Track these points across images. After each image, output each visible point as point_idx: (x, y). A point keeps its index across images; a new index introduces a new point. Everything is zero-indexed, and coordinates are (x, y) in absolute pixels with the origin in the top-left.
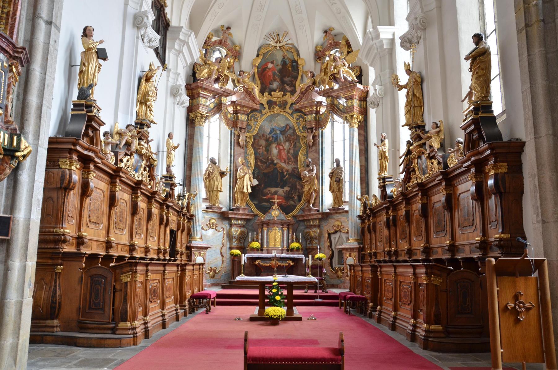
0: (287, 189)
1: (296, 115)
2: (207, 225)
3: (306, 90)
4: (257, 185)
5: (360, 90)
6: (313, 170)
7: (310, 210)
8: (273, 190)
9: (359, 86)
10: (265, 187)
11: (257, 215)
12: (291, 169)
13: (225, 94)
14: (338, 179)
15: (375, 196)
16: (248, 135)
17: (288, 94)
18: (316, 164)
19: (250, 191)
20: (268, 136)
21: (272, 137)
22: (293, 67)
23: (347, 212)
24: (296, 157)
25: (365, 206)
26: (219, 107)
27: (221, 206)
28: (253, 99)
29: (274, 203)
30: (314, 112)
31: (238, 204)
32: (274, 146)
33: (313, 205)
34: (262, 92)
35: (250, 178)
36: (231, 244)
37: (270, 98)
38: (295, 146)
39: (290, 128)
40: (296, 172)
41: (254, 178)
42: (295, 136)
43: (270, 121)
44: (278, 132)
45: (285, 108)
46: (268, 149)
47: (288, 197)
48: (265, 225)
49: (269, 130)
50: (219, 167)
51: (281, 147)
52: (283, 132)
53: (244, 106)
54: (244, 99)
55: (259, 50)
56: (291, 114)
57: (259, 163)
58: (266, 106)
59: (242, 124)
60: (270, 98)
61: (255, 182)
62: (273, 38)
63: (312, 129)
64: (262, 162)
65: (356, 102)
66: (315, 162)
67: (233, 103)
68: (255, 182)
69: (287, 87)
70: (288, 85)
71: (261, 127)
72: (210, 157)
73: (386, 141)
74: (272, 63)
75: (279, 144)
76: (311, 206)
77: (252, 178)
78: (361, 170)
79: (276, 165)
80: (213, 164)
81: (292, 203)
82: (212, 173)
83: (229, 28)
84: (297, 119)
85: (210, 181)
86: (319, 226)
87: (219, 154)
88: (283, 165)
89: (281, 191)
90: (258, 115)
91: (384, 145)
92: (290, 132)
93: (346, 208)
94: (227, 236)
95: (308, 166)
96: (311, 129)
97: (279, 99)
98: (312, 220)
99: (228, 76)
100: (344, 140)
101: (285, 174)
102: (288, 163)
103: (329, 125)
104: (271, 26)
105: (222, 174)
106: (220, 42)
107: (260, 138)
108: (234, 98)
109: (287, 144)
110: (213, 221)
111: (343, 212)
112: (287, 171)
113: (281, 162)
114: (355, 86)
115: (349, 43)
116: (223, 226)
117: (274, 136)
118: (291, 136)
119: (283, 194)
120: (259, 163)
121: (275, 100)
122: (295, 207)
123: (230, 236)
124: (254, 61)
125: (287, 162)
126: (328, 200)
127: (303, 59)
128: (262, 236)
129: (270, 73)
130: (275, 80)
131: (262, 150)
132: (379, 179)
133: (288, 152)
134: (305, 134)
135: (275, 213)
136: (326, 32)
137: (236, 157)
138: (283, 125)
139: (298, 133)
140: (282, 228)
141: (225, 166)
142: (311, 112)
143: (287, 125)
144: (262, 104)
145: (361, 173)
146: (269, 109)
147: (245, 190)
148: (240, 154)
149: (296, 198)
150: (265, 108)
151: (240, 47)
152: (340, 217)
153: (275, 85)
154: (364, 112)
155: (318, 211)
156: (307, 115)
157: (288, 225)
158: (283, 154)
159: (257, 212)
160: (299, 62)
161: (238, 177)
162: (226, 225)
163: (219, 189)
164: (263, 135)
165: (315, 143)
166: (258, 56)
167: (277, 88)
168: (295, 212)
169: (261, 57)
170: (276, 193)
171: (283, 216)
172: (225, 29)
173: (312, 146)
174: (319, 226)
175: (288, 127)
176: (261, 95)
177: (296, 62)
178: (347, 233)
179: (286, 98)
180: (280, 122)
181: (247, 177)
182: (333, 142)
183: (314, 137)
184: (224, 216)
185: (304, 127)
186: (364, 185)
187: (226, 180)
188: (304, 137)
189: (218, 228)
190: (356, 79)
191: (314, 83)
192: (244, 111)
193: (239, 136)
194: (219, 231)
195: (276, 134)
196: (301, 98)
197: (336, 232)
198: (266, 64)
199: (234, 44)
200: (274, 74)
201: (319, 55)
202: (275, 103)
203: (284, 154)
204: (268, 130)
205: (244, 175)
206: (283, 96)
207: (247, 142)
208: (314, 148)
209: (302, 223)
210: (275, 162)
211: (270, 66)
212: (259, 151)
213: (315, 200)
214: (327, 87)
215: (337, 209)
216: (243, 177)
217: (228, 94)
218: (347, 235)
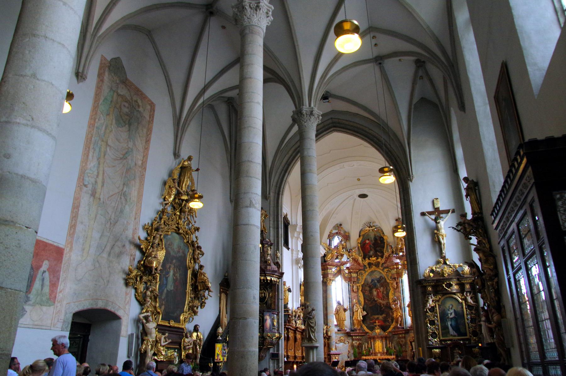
0: (384, 315)
1: (385, 270)
6: (397, 304)
8: (376, 317)
10: (371, 315)
11: (368, 332)
16: (358, 285)
19: (362, 319)
26: (340, 272)
27: (346, 329)
28: (359, 264)
29: (376, 326)
31: (356, 327)
32: (374, 290)
33: (400, 325)
34: (364, 258)
38: (387, 289)
46: (371, 292)
47: (385, 320)
50: (343, 306)
52: (379, 281)
54: (353, 265)
55: (360, 232)
56: (383, 270)
58: (367, 266)
60: (369, 261)
61: (365, 313)
64: (368, 300)
66: (398, 298)
67: (347, 268)
68: (365, 313)
69: (379, 254)
71: (365, 280)
72: (338, 300)
74: (368, 240)
75: (377, 289)
79: (376, 301)
81: (388, 324)
83: (341, 225)
86: (405, 337)
88: (381, 301)
89: (381, 317)
90: (363, 272)
95: (395, 301)
96: (395, 278)
98: (401, 334)
104: (365, 220)
105: (345, 310)
106: (337, 233)
108: (348, 265)
112: (383, 305)
123: (352, 346)
124: (358, 240)
130: (371, 250)
131: (367, 293)
133: (383, 293)
134: (392, 282)
135: (378, 331)
136: (397, 220)
138: (378, 277)
139: (388, 281)
141: (346, 305)
142: (394, 268)
143: (381, 277)
151: (349, 233)
153: (371, 253)
155: (403, 328)
159: (367, 330)
160: (385, 238)
164: (367, 284)
165: (398, 287)
166: (360, 236)
168: (390, 329)
169: (361, 237)
170: (378, 319)
171: (382, 333)
174: (405, 337)
177: (383, 238)
181: (359, 310)
183: (397, 283)
184: (348, 335)
185: (391, 277)
187: (348, 313)
191: (393, 252)
195: (375, 283)
196: (386, 261)
198: (365, 241)
199: (345, 232)
200: (370, 246)
202: (372, 264)
203: (380, 294)
206: (377, 259)
207: (358, 289)
208: (398, 290)
209: (395, 336)
211: (367, 242)
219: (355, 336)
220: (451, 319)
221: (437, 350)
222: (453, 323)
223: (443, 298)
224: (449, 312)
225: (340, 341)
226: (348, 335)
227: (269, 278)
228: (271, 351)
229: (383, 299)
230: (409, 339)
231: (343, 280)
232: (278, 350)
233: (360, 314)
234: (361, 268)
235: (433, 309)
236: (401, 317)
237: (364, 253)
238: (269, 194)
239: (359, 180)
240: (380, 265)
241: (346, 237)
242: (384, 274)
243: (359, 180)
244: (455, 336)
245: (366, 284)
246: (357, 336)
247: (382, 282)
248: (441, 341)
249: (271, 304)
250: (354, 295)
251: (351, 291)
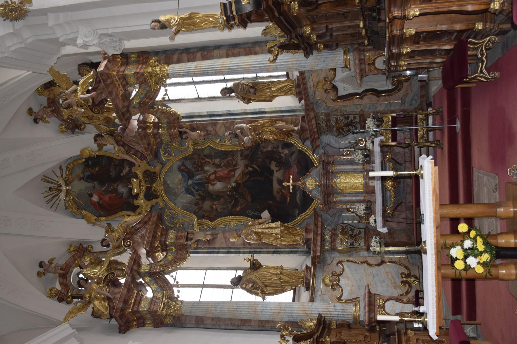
0: (273, 166)
2: (334, 289)
3: (124, 145)
4: (269, 212)
5: (110, 65)
6: (242, 129)
7: (303, 130)
8: (276, 186)
9: (101, 68)
12: (244, 161)
13: (135, 267)
14: (252, 90)
15: (265, 33)
17: (134, 170)
18: (233, 124)
19: (278, 223)
20: (198, 197)
21: (197, 191)
23: (302, 73)
24: (225, 154)
25: (284, 47)
26: (157, 277)
27: (304, 267)
30: (155, 131)
32: (210, 188)
34: (134, 209)
35: (260, 224)
37: (142, 196)
38: (209, 156)
39: (183, 165)
40: (247, 152)
41: (261, 218)
42: (195, 156)
43: (175, 194)
44: (190, 182)
45: (154, 173)
46: (216, 196)
47: (284, 164)
48: (331, 199)
49: (188, 196)
51: (212, 177)
52: (189, 174)
53: (154, 237)
56: (163, 164)
57: (238, 209)
58: (154, 201)
59: (181, 237)
60: (142, 196)
61: (266, 214)
62: (54, 197)
63: (181, 133)
64: (235, 205)
65: (130, 71)
66: (229, 125)
67: (150, 254)
68: (266, 214)
70: (122, 172)
73: (162, 18)
74: (91, 196)
75: (208, 181)
76: (296, 128)
77: (260, 221)
78: (234, 55)
79: (238, 184)
80: (242, 282)
82: (254, 283)
84: (170, 155)
85: (266, 286)
87: (227, 269)
88: (238, 173)
89: (277, 175)
91: (168, 21)
92: (188, 164)
93: (296, 74)
94: (350, 256)
96: (181, 133)
97: (143, 183)
98: (318, 125)
99: (110, 263)
100: (194, 83)
101: (251, 169)
102: (236, 165)
103: (175, 108)
105: (256, 266)
107: (200, 208)
108: (143, 251)
109: (206, 168)
110: (327, 281)
111: (304, 79)
112: (246, 166)
113: (234, 176)
114: (102, 73)
115: (45, 84)
116: (335, 262)
117: (196, 188)
118: (194, 163)
119: (282, 171)
120: (238, 209)
121: (144, 188)
122: (301, 152)
124: (89, 222)
125: (233, 168)
126: (287, 102)
127: (82, 151)
128: (346, 202)
129: (106, 198)
130: (116, 190)
131: (218, 206)
132: (231, 27)
133: (218, 166)
135: (310, 183)
136: (36, 121)
137: (230, 245)
138: (180, 176)
140: (332, 172)
142: (156, 135)
143: (180, 169)
144: (152, 207)
145: (239, 55)
146: (157, 197)
148: (225, 238)
149: (286, 151)
150: (157, 203)
152: (310, 84)
153: (122, 189)
154: (144, 56)
156: (161, 141)
157: (328, 163)
158: (221, 174)
159: (310, 210)
160: (87, 154)
161: (258, 242)
162: (334, 258)
163: (278, 272)
164: (196, 204)
165: (202, 127)
167: (127, 186)
169: (84, 212)
170: (280, 182)
171: (314, 172)
172: (42, 270)
173: (207, 131)
175: (182, 168)
176: (138, 210)
178: (335, 70)
179: (140, 175)
180: (176, 179)
181: (258, 229)
182: (199, 99)
183: (193, 129)
184: (318, 262)
186: (257, 49)
187: (266, 260)
188: (195, 143)
189: (338, 270)
190: (92, 72)
192: (162, 235)
193: (198, 241)
194: (343, 270)
195: (193, 185)
197: (335, 88)
198: (94, 204)
201: (73, 126)
202: (148, 189)
203: (222, 173)
204: (188, 197)
205: (255, 233)
206: (137, 178)
208: (210, 128)
210: (234, 185)
211: (95, 198)
212: (219, 210)
213: (287, 122)
214: (114, 115)
215: (300, 87)
216: (257, 234)
217: (136, 260)
218: (339, 71)
219: (322, 246)
225: (335, 285)
226: (318, 262)
230: (331, 104)
231: (185, 264)
233: (269, 228)
234: (154, 219)
236: (274, 120)
237: (122, 210)
240: (152, 169)
241: (80, 250)
242: (174, 162)
245: (196, 208)
246: (323, 239)
247: (193, 165)
250: (220, 241)
251: (210, 247)
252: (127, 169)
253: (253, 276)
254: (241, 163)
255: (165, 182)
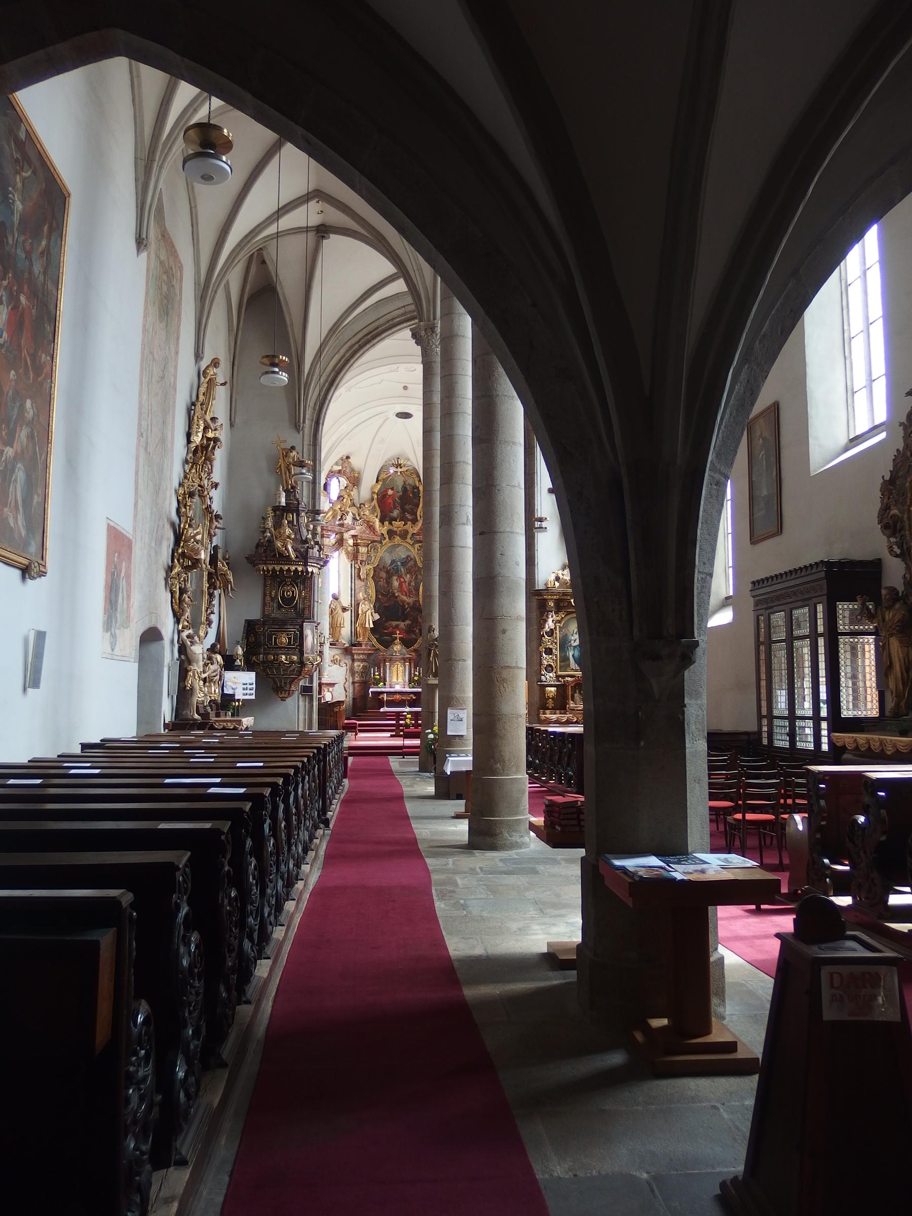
0: (408, 622)
1: (417, 546)
8: (394, 623)
10: (386, 621)
16: (368, 567)
17: (409, 523)
19: (372, 626)
22: (414, 493)
29: (396, 638)
32: (395, 578)
34: (382, 521)
36: (353, 679)
37: (391, 527)
38: (416, 578)
43: (391, 552)
46: (389, 582)
47: (409, 630)
52: (404, 564)
54: (364, 532)
56: (413, 545)
58: (387, 536)
60: (391, 527)
61: (377, 617)
64: (382, 595)
67: (354, 537)
68: (377, 617)
74: (392, 489)
75: (400, 577)
83: (348, 457)
88: (404, 598)
89: (402, 625)
90: (379, 545)
92: (412, 563)
106: (339, 472)
109: (408, 576)
110: (337, 657)
112: (408, 604)
121: (395, 529)
123: (352, 672)
129: (390, 501)
130: (395, 508)
131: (382, 583)
133: (409, 584)
135: (397, 647)
141: (346, 601)
143: (408, 556)
146: (390, 539)
147: (367, 626)
151: (359, 473)
153: (396, 513)
159: (378, 646)
161: (360, 612)
164: (384, 567)
166: (377, 481)
170: (397, 627)
179: (406, 527)
180: (402, 553)
181: (369, 613)
184: (347, 651)
193: (359, 569)
195: (397, 566)
198: (386, 491)
199: (353, 470)
200: (395, 501)
202: (395, 533)
220: (575, 647)
221: (553, 689)
222: (577, 654)
223: (568, 617)
224: (573, 638)
225: (334, 662)
227: (310, 569)
228: (301, 683)
229: (409, 594)
232: (311, 681)
234: (376, 538)
235: (551, 633)
238: (304, 422)
239: (405, 388)
240: (409, 536)
241: (355, 481)
243: (405, 388)
244: (576, 671)
248: (558, 677)
249: (304, 609)
250: (358, 582)
252: (410, 518)
253: (339, 610)
254: (410, 600)
255: (399, 545)
